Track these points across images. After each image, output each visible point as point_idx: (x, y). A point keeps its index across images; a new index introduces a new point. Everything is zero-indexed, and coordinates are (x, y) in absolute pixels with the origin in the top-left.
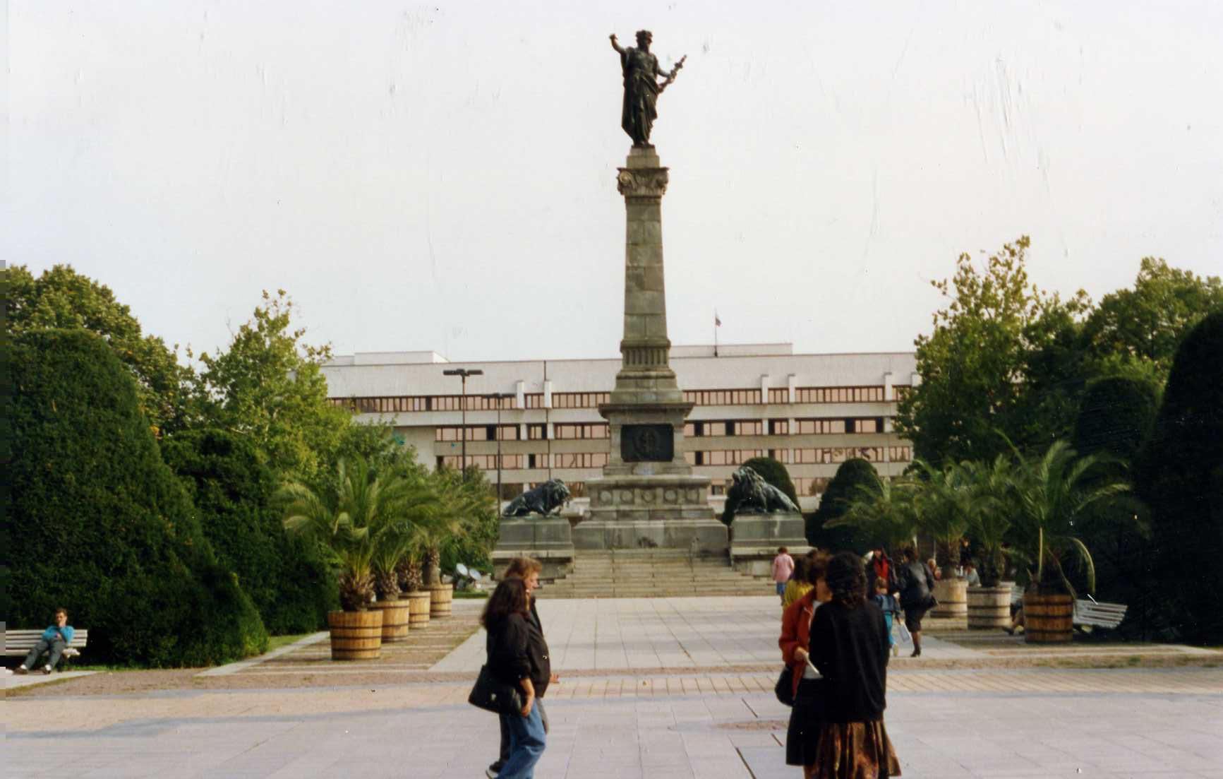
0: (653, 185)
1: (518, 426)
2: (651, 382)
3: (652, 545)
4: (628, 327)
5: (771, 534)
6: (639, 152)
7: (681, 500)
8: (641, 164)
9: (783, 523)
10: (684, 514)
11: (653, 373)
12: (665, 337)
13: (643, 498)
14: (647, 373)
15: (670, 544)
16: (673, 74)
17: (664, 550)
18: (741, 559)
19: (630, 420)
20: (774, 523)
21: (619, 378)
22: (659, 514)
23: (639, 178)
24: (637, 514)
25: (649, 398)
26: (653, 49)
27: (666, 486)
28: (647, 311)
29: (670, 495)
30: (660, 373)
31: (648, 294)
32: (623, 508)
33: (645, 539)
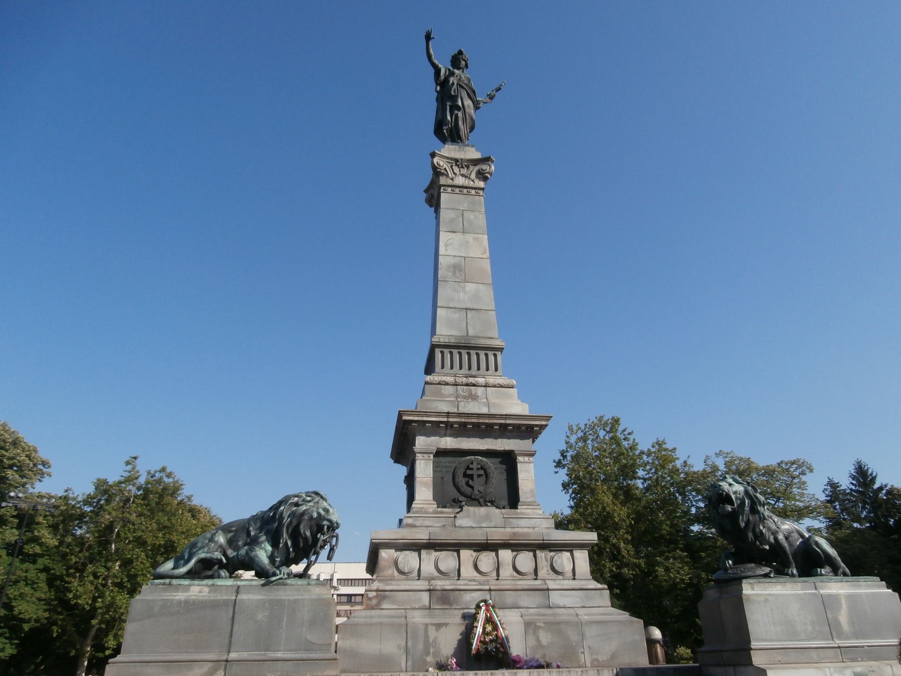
0: (473, 176)
2: (480, 391)
5: (833, 629)
7: (544, 572)
11: (481, 381)
13: (476, 567)
14: (471, 380)
19: (449, 442)
20: (835, 598)
22: (510, 598)
23: (456, 169)
29: (525, 560)
30: (491, 380)
31: (470, 287)
32: (440, 584)
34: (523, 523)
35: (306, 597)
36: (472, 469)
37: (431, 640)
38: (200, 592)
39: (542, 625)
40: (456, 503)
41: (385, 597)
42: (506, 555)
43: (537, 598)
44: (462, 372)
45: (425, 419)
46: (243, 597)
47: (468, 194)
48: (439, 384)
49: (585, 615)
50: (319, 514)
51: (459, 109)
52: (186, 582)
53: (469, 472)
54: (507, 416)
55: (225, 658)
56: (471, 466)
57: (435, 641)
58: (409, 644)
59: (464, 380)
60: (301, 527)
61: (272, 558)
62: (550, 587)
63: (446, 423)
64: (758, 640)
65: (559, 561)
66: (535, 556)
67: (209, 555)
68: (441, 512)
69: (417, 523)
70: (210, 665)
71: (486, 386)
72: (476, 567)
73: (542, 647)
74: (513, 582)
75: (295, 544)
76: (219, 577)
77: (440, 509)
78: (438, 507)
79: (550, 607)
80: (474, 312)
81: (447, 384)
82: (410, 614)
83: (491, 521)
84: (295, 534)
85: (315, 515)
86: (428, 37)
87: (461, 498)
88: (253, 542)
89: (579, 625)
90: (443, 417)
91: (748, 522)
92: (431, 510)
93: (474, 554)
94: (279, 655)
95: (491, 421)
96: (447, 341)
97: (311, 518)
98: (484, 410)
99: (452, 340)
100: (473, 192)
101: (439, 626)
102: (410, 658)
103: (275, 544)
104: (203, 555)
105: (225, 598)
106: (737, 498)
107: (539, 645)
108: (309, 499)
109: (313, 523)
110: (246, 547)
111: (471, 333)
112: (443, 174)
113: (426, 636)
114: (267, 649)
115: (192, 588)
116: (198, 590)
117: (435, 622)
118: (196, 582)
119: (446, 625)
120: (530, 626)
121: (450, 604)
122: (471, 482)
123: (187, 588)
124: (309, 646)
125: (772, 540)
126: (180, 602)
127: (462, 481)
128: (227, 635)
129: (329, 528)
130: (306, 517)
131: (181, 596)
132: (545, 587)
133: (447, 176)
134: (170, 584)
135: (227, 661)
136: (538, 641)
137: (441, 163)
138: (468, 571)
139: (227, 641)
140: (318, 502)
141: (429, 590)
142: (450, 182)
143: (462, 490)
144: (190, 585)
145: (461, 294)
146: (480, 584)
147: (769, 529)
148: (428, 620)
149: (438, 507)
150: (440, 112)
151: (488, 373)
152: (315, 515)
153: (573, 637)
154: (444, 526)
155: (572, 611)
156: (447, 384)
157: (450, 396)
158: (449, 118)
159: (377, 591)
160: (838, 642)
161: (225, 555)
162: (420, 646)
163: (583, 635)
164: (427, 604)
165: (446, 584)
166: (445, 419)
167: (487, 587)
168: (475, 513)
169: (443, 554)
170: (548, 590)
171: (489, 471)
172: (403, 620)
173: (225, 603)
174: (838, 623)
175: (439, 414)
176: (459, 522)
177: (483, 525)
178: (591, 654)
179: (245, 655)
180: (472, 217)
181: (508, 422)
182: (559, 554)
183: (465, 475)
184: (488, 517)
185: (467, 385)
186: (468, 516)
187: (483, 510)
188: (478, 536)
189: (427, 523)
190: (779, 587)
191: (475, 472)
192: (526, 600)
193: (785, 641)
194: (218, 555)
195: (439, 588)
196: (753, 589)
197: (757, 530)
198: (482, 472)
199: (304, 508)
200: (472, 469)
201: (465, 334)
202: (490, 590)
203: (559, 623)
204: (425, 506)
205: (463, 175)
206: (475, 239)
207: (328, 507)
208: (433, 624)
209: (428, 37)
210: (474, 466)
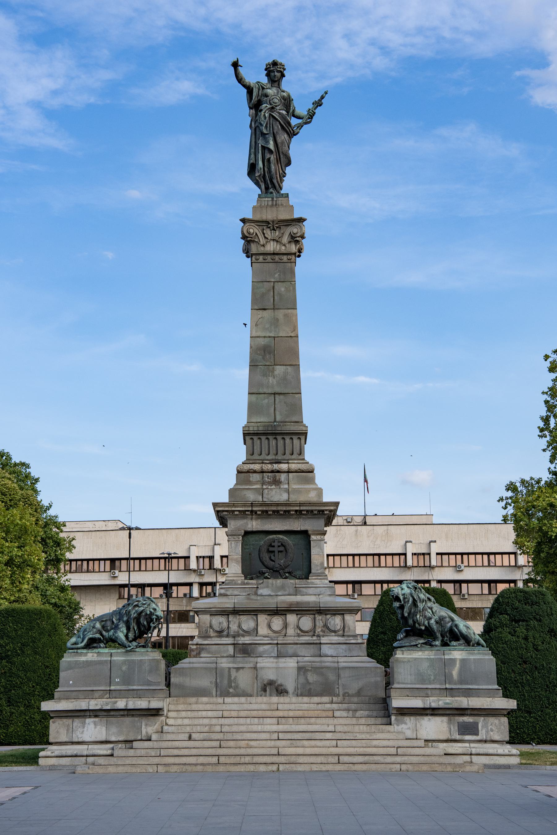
0: (285, 239)
1: (190, 585)
2: (283, 477)
3: (281, 691)
4: (253, 409)
5: (447, 678)
6: (267, 200)
8: (269, 215)
9: (463, 661)
10: (326, 649)
11: (284, 467)
12: (300, 422)
13: (269, 627)
14: (276, 467)
15: (306, 691)
16: (311, 115)
17: (294, 699)
18: (403, 712)
19: (254, 525)
20: (453, 661)
21: (239, 472)
22: (291, 649)
23: (268, 232)
24: (261, 649)
25: (277, 495)
26: (285, 84)
27: (300, 610)
28: (278, 390)
29: (306, 622)
30: (293, 467)
31: (279, 370)
33: (271, 683)
34: (311, 591)
35: (146, 658)
36: (274, 546)
37: (232, 678)
38: (93, 656)
39: (310, 669)
40: (261, 575)
41: (203, 649)
42: (292, 618)
43: (312, 650)
44: (269, 457)
45: (233, 509)
46: (114, 658)
47: (281, 262)
48: (248, 472)
49: (343, 662)
50: (151, 612)
51: (271, 151)
52: (85, 651)
53: (271, 549)
54: (301, 504)
55: (109, 689)
56: (273, 544)
57: (235, 679)
58: (218, 681)
59: (269, 467)
60: (141, 619)
61: (127, 636)
62: (322, 642)
63: (252, 511)
64: (399, 683)
65: (332, 622)
66: (315, 619)
67: (94, 636)
68: (247, 584)
69: (228, 593)
70: (102, 692)
71: (288, 472)
72: (269, 627)
73: (310, 683)
74: (296, 638)
75: (139, 628)
76: (100, 647)
77: (246, 581)
78: (246, 578)
79: (320, 656)
80: (282, 397)
81: (255, 472)
82: (219, 660)
83: (285, 591)
84: (138, 623)
85: (148, 612)
86: (235, 65)
87: (264, 570)
88: (116, 628)
89: (337, 670)
90: (248, 506)
91: (409, 614)
92: (240, 582)
93: (269, 617)
94: (135, 687)
95: (288, 509)
96: (256, 429)
97: (146, 614)
98: (284, 497)
99: (261, 429)
100: (285, 258)
101: (238, 669)
102: (218, 689)
103: (128, 629)
104: (91, 636)
105: (105, 659)
106: (404, 598)
107: (308, 682)
108: (144, 602)
109: (147, 617)
110: (112, 631)
111: (278, 418)
112: (254, 241)
113: (230, 676)
114: (129, 684)
115: (88, 654)
116: (91, 656)
117: (236, 666)
118: (90, 651)
119: (243, 668)
120: (301, 670)
121: (248, 653)
122: (273, 558)
123: (86, 654)
124: (149, 683)
125: (426, 623)
126: (84, 661)
127: (266, 557)
128: (109, 678)
129: (156, 619)
130: (144, 614)
131: (83, 659)
132: (318, 642)
133: (258, 243)
134: (77, 652)
135: (110, 690)
136: (307, 680)
137: (251, 231)
138: (263, 630)
139: (109, 680)
140: (149, 605)
141: (234, 644)
142: (262, 250)
143: (266, 563)
144: (87, 653)
145: (271, 379)
146: (272, 640)
147: (425, 617)
148: (231, 665)
149: (246, 578)
150: (253, 156)
151: (293, 457)
152: (148, 612)
153: (332, 677)
154: (249, 594)
155: (335, 659)
156: (255, 472)
157: (256, 483)
158: (261, 164)
159: (197, 644)
160: (448, 686)
161: (101, 635)
162: (226, 682)
163: (339, 676)
164: (232, 653)
165: (246, 640)
166: (250, 509)
167: (276, 642)
168: (272, 584)
169: (243, 618)
170: (320, 644)
171: (288, 547)
172: (214, 666)
173: (106, 661)
174: (451, 675)
175: (244, 505)
176: (260, 592)
177: (279, 593)
178: (344, 689)
179: (118, 688)
180: (283, 289)
181: (302, 508)
182: (333, 617)
183: (269, 552)
184: (283, 587)
185: (272, 472)
186: (268, 587)
187: (279, 582)
188: (271, 603)
189: (236, 592)
190: (420, 653)
191: (276, 549)
192: (302, 650)
193: (415, 684)
194: (98, 636)
195: (240, 642)
196: (403, 654)
197: (415, 618)
198: (282, 549)
199: (142, 609)
200: (274, 546)
201: (273, 420)
202: (277, 644)
203: (322, 668)
204: (235, 578)
205: (273, 240)
206: (286, 315)
207: (155, 607)
208: (235, 668)
209: (235, 65)
210: (276, 544)
